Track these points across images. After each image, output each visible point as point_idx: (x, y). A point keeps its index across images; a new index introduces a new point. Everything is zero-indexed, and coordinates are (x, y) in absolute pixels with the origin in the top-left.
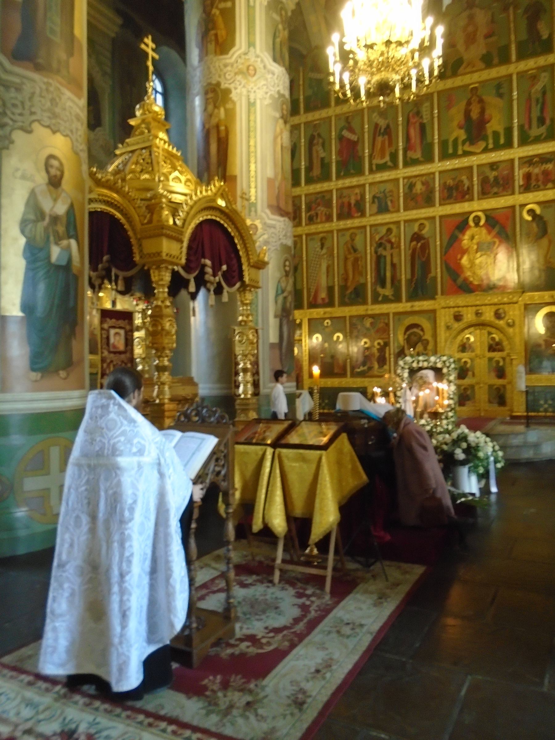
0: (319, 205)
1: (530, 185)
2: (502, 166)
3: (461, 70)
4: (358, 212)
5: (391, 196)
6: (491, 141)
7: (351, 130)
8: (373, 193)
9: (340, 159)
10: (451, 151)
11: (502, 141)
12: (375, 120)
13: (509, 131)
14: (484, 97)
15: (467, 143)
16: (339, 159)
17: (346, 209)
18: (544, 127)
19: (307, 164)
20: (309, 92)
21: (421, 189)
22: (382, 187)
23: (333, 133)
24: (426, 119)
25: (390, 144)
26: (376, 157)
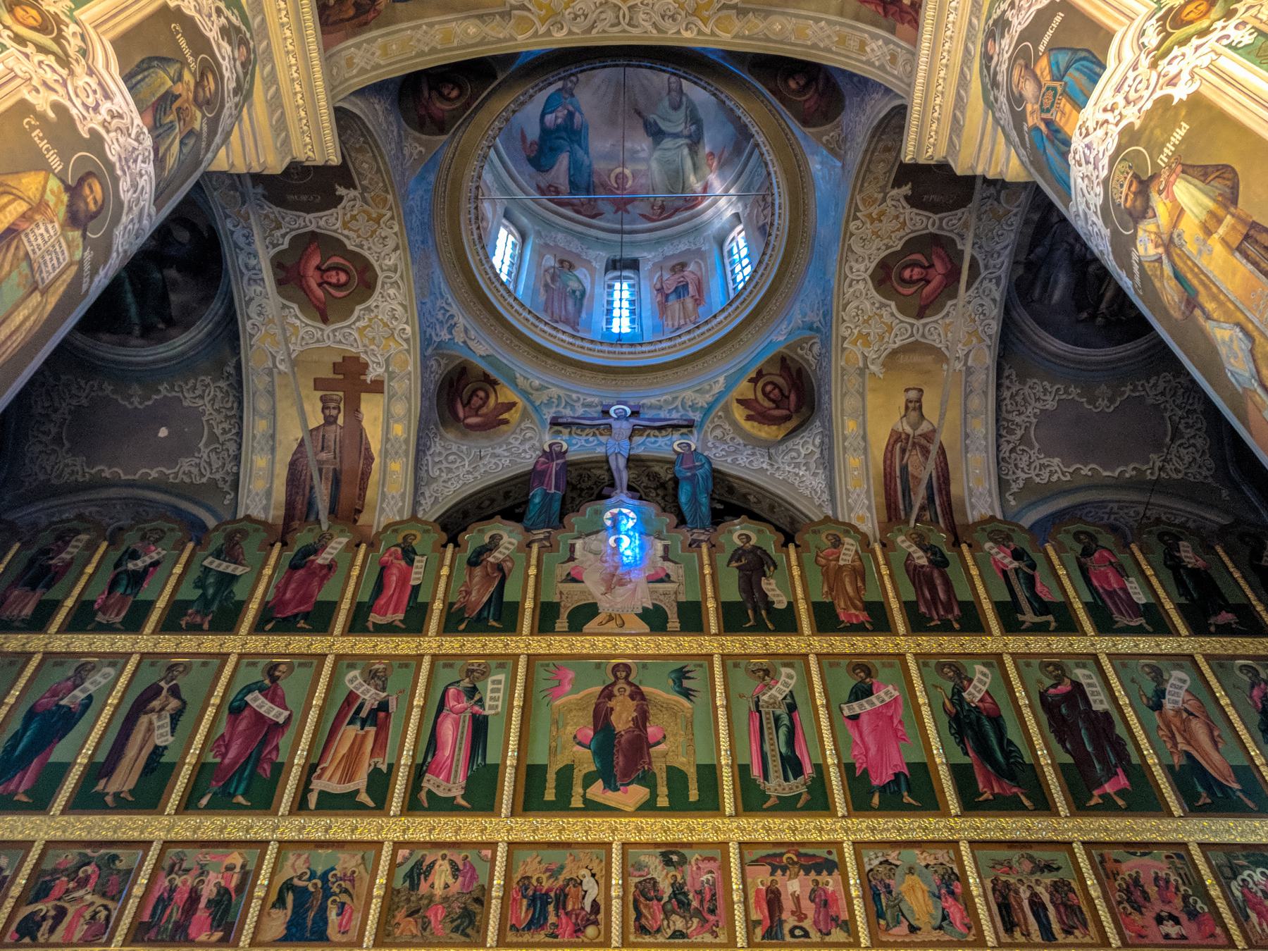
0: (83, 883)
1: (781, 922)
2: (693, 856)
3: (591, 626)
4: (214, 927)
5: (346, 891)
6: (663, 790)
7: (274, 695)
8: (287, 873)
9: (218, 760)
10: (550, 795)
11: (694, 795)
12: (351, 687)
13: (709, 775)
14: (645, 689)
15: (599, 784)
16: (210, 758)
17: (175, 913)
18: (801, 779)
19: (101, 758)
20: (189, 593)
21: (447, 886)
22: (321, 862)
23: (219, 691)
24: (491, 707)
25: (380, 744)
26: (328, 774)
